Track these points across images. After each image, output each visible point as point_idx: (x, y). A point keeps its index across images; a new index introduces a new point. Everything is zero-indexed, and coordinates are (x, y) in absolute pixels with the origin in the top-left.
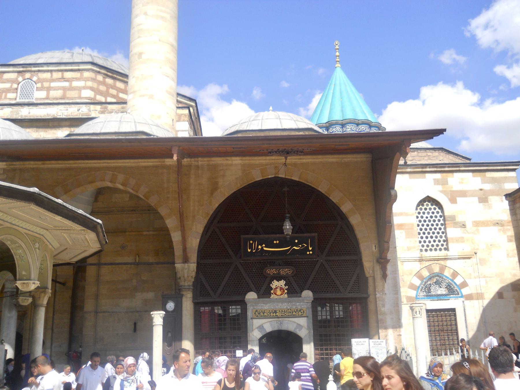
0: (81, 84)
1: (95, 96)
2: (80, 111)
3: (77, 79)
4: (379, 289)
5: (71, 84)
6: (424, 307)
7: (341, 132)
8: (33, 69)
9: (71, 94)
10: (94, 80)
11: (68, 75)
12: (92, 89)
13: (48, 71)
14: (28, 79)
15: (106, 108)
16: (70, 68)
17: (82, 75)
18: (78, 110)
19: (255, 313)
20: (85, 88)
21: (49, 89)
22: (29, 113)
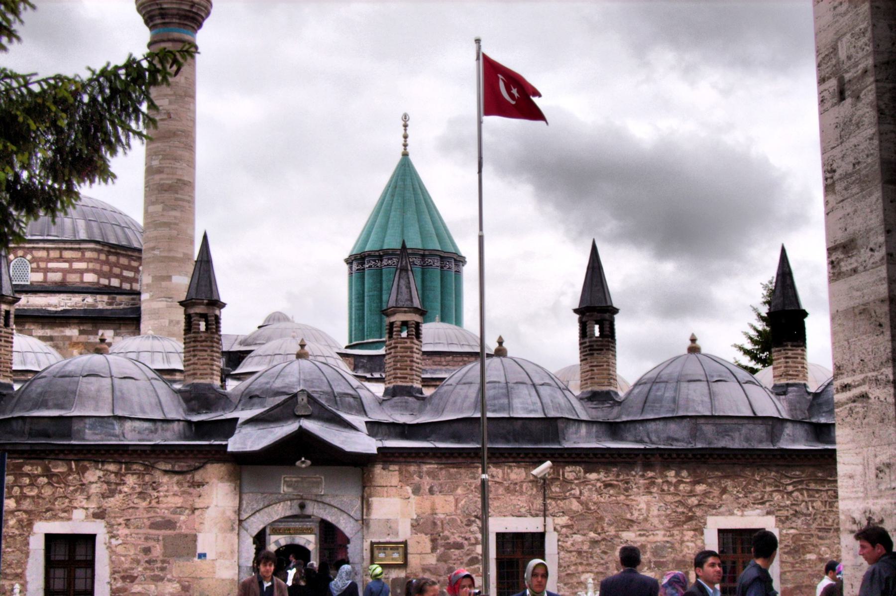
0: (82, 265)
1: (99, 279)
2: (85, 302)
5: (71, 266)
9: (73, 278)
10: (96, 260)
11: (67, 254)
12: (94, 271)
13: (44, 249)
15: (114, 299)
16: (70, 246)
17: (83, 255)
18: (83, 300)
20: (87, 271)
21: (46, 271)
22: (28, 302)
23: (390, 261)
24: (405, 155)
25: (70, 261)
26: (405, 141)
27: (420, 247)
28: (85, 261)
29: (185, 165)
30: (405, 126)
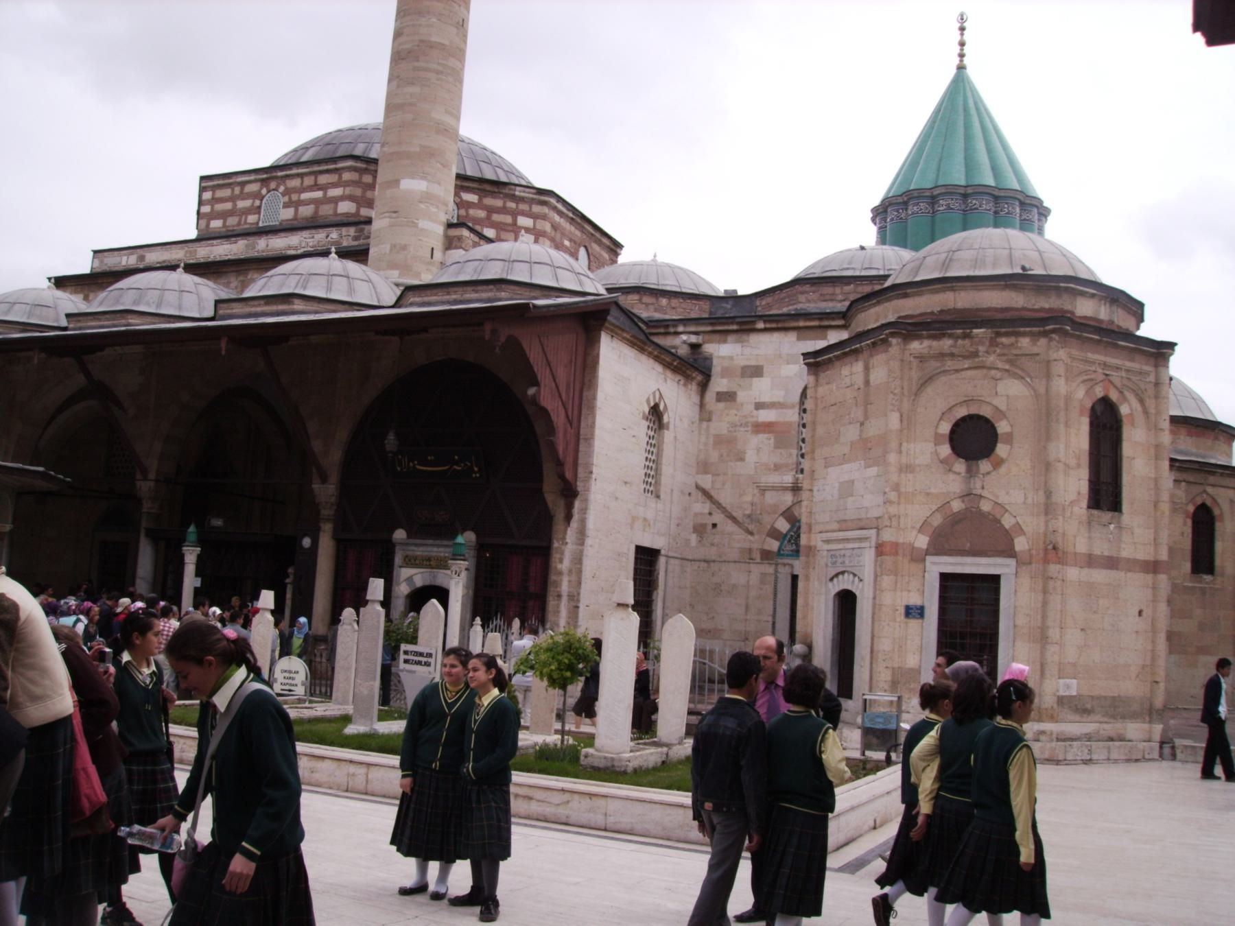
1: (358, 209)
2: (329, 238)
3: (334, 185)
4: (556, 536)
5: (325, 194)
6: (787, 570)
7: (928, 213)
8: (280, 174)
9: (326, 210)
11: (323, 179)
12: (351, 198)
14: (274, 190)
15: (362, 230)
17: (340, 177)
18: (327, 236)
19: (405, 560)
20: (342, 198)
22: (267, 246)
23: (915, 208)
24: (961, 68)
25: (324, 188)
26: (962, 50)
27: (963, 183)
28: (341, 186)
29: (435, 20)
30: (962, 29)
